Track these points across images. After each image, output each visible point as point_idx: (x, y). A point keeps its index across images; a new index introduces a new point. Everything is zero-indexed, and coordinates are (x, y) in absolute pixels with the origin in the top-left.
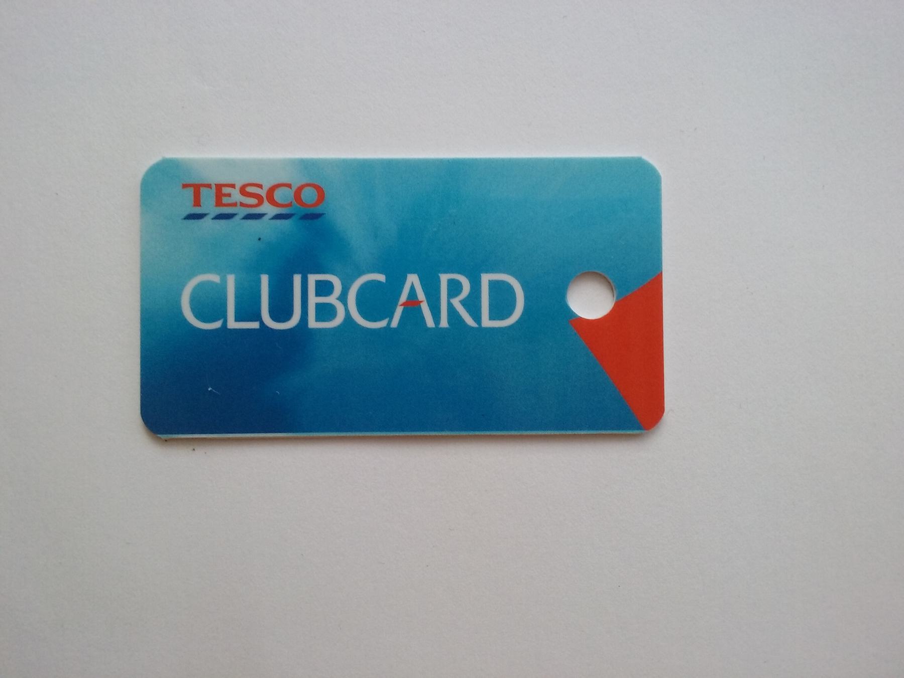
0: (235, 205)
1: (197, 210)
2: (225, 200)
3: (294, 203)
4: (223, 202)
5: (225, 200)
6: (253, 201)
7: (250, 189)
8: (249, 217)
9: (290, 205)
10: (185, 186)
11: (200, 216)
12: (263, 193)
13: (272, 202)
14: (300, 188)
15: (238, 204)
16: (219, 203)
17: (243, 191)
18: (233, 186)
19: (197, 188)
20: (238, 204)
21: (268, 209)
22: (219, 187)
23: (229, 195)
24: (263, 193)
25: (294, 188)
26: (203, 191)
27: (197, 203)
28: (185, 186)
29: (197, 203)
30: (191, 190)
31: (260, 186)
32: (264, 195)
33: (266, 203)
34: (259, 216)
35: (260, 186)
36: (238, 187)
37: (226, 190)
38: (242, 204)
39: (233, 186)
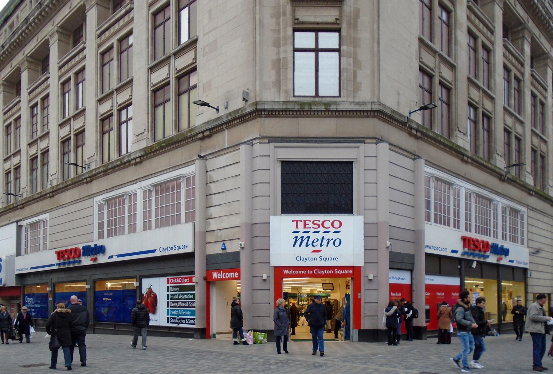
0: (310, 228)
1: (297, 230)
4: (306, 227)
6: (317, 226)
7: (315, 222)
8: (315, 232)
9: (329, 228)
10: (293, 221)
11: (298, 232)
12: (320, 223)
15: (312, 228)
16: (305, 227)
18: (310, 221)
19: (297, 222)
20: (312, 228)
21: (322, 229)
22: (305, 221)
23: (308, 224)
24: (320, 223)
25: (331, 222)
27: (297, 227)
28: (293, 221)
29: (297, 227)
30: (295, 222)
31: (319, 221)
34: (318, 232)
35: (319, 221)
36: (312, 221)
37: (307, 223)
38: (313, 228)
39: (310, 221)
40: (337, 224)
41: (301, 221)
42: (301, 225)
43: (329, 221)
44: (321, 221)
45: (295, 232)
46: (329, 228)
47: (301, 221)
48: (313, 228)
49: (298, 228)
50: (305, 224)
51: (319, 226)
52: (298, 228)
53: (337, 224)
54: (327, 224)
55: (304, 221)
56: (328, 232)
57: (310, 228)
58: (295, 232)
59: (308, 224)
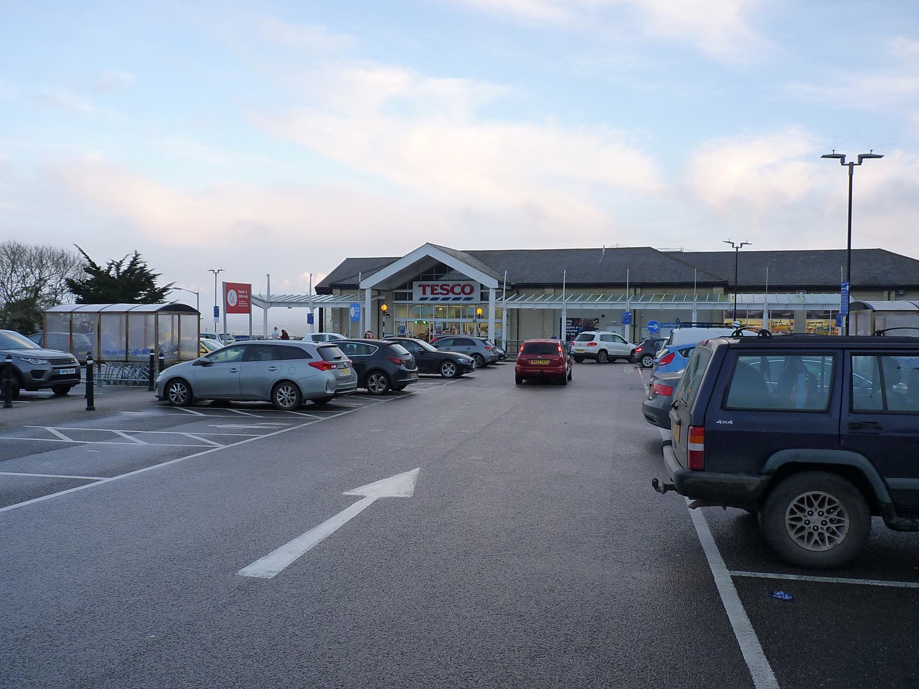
0: (438, 294)
1: (425, 296)
2: (435, 292)
3: (462, 294)
5: (435, 292)
6: (445, 292)
7: (444, 287)
9: (459, 294)
10: (420, 286)
12: (449, 288)
16: (432, 293)
21: (451, 295)
23: (436, 290)
24: (449, 288)
26: (427, 288)
27: (424, 293)
29: (424, 293)
31: (448, 286)
32: (449, 289)
37: (435, 288)
38: (441, 294)
40: (467, 290)
41: (429, 286)
42: (428, 290)
45: (421, 299)
46: (459, 294)
48: (441, 294)
49: (425, 294)
51: (447, 294)
52: (425, 294)
53: (467, 290)
54: (457, 290)
56: (459, 299)
57: (438, 294)
58: (421, 299)
59: (436, 290)
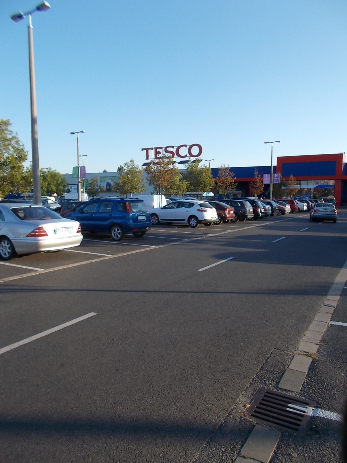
3: (188, 155)
7: (169, 149)
9: (186, 156)
10: (143, 150)
12: (174, 150)
13: (179, 156)
14: (191, 147)
17: (166, 151)
18: (161, 148)
19: (147, 150)
22: (156, 149)
24: (174, 150)
25: (188, 147)
26: (149, 150)
27: (147, 158)
28: (143, 150)
29: (147, 158)
30: (145, 151)
31: (173, 147)
33: (175, 156)
35: (173, 147)
36: (164, 149)
37: (158, 150)
39: (161, 148)
40: (195, 151)
41: (152, 149)
43: (186, 146)
44: (176, 148)
46: (186, 156)
47: (152, 149)
50: (157, 153)
51: (173, 156)
53: (195, 151)
54: (183, 151)
55: (155, 148)
